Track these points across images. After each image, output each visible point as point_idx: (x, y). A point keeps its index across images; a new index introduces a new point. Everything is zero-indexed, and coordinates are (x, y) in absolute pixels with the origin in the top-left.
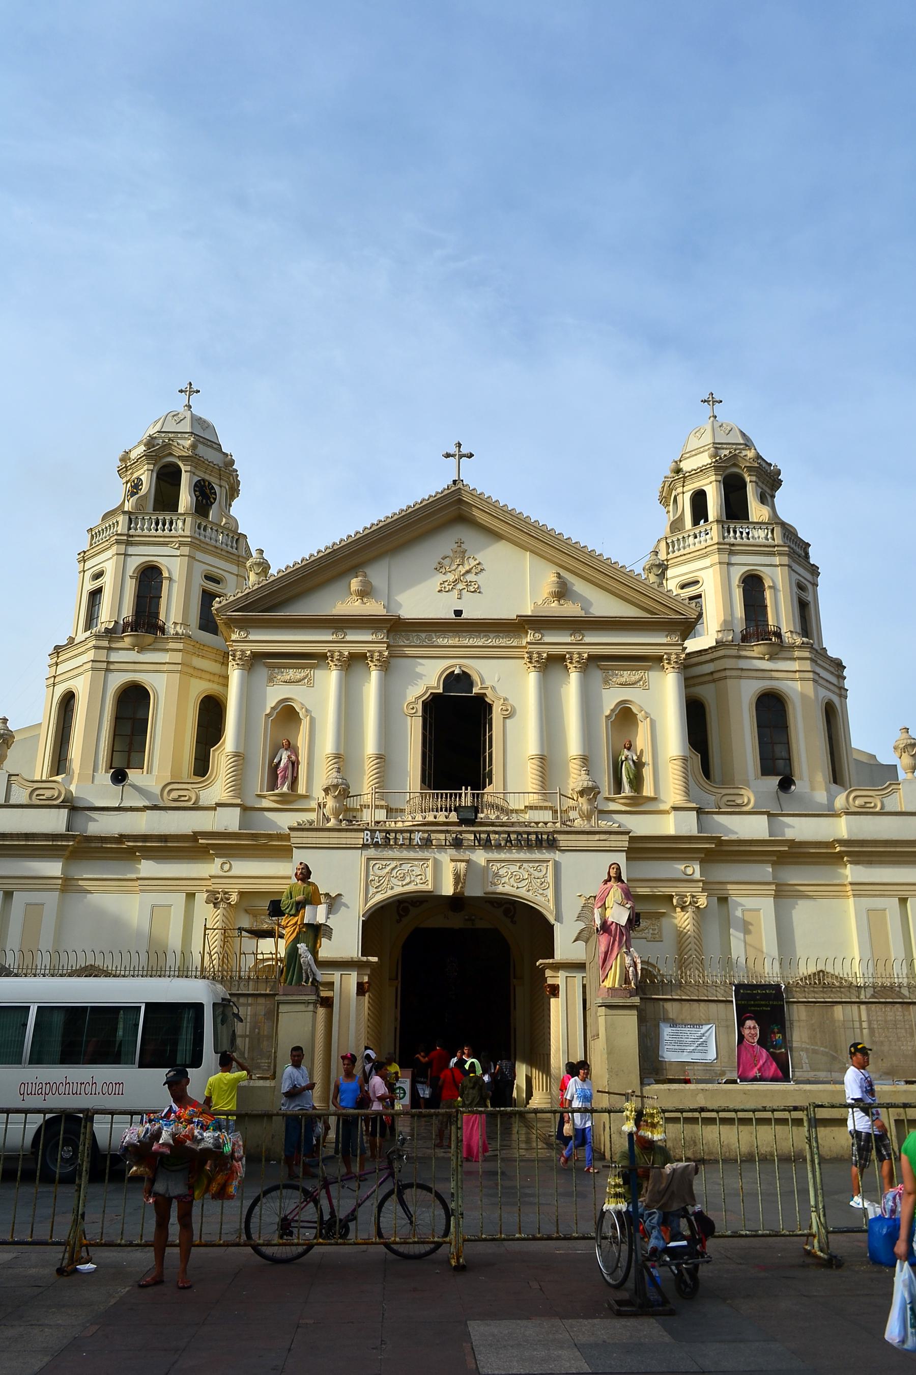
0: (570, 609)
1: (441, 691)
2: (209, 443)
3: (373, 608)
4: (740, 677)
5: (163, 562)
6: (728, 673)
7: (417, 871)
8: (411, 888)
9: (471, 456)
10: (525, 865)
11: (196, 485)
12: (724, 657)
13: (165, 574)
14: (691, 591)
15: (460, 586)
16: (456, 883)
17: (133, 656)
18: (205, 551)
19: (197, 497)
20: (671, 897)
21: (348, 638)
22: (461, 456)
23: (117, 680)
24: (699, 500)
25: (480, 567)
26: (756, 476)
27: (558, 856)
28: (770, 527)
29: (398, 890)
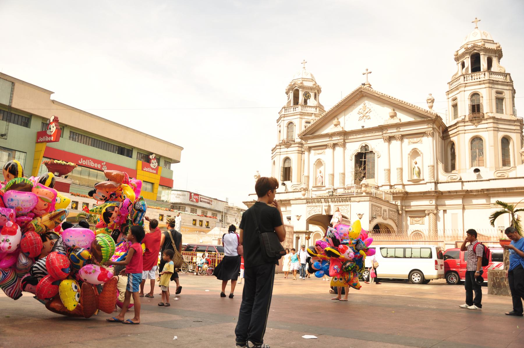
0: (395, 121)
1: (360, 152)
2: (308, 80)
3: (339, 129)
4: (465, 133)
5: (293, 121)
6: (460, 132)
7: (318, 209)
8: (316, 214)
9: (370, 73)
10: (343, 206)
11: (304, 94)
12: (459, 126)
13: (294, 125)
14: (455, 102)
15: (365, 118)
16: (326, 212)
17: (286, 150)
18: (305, 115)
19: (304, 98)
20: (425, 211)
21: (333, 139)
22: (368, 73)
23: (283, 157)
24: (463, 65)
25: (370, 111)
26: (483, 52)
27: (352, 203)
28: (483, 73)
29: (314, 214)
